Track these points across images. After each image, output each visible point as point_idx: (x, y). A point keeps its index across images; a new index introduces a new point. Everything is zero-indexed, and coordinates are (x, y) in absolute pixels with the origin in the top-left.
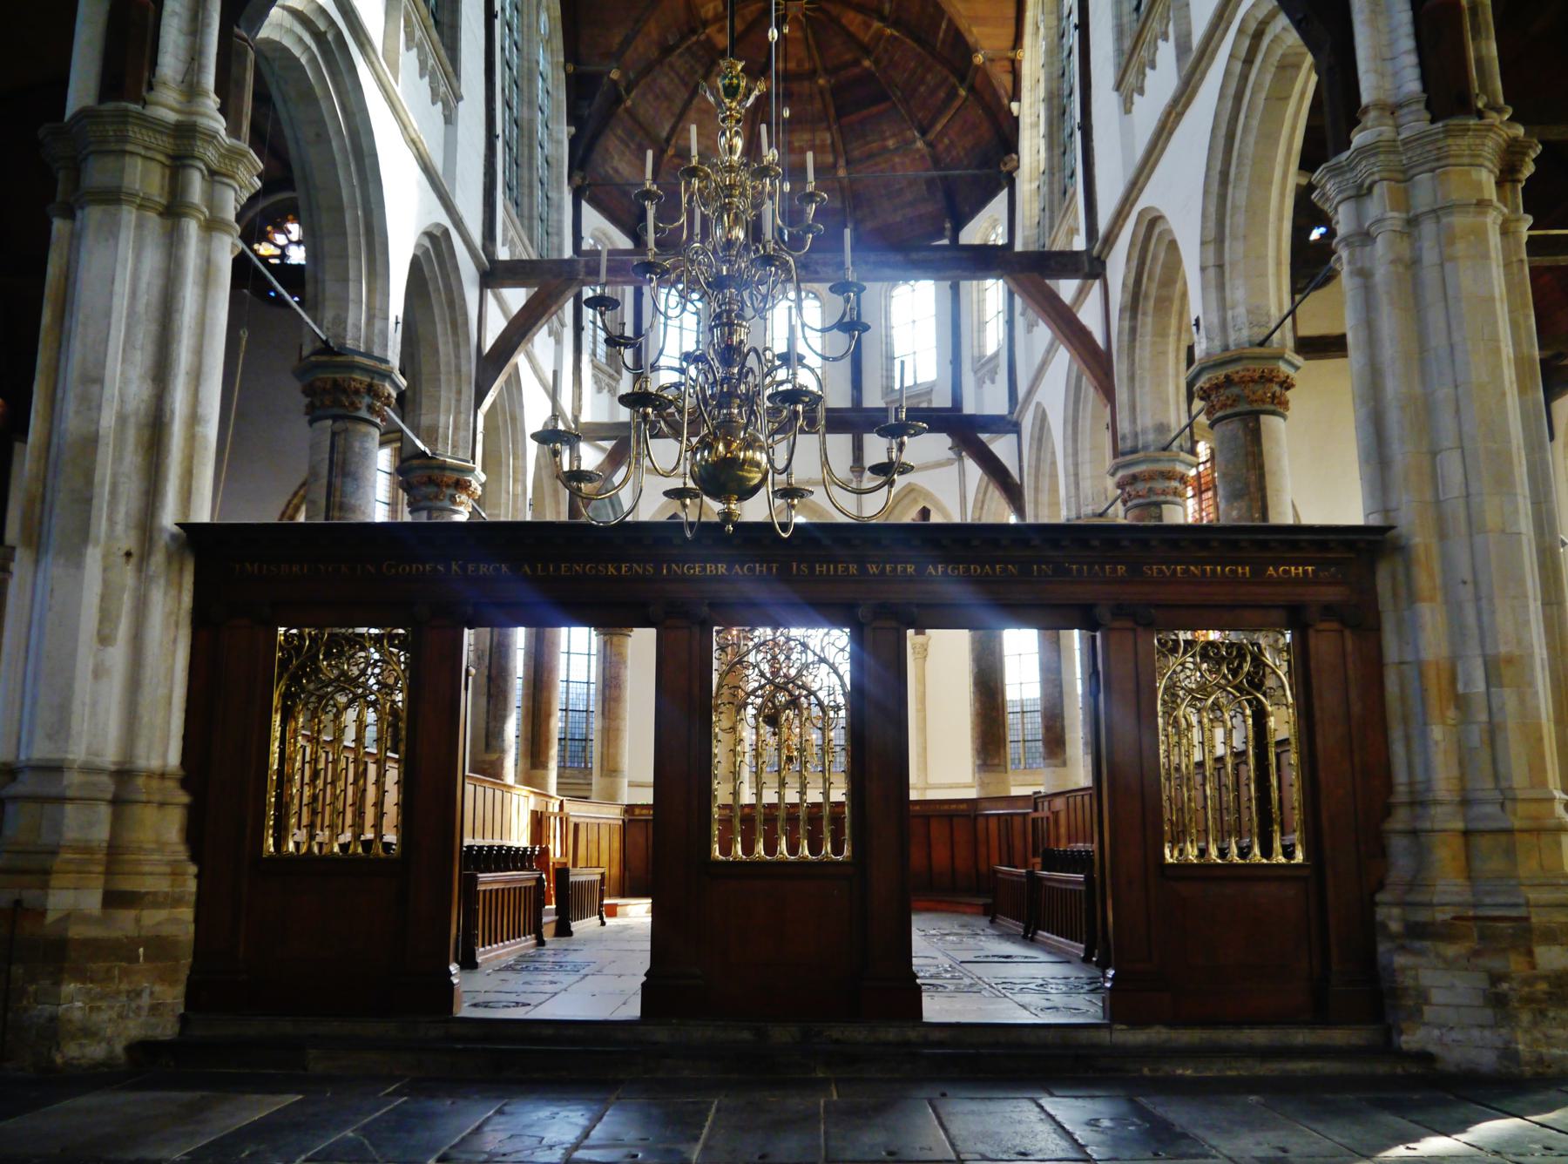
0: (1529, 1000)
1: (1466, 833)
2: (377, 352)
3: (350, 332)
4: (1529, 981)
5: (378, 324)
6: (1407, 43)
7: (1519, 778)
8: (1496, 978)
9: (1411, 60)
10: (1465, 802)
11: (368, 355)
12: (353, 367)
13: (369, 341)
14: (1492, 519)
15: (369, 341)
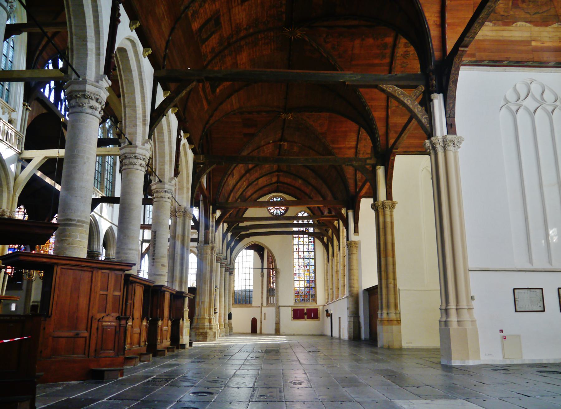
0: (198, 335)
1: (198, 319)
2: (98, 251)
3: (94, 249)
4: (199, 333)
5: (99, 247)
6: (204, 235)
7: (202, 313)
8: (196, 333)
9: (204, 237)
10: (198, 316)
11: (97, 252)
12: (95, 254)
13: (97, 250)
14: (203, 287)
15: (97, 250)
